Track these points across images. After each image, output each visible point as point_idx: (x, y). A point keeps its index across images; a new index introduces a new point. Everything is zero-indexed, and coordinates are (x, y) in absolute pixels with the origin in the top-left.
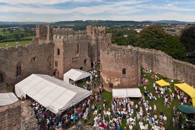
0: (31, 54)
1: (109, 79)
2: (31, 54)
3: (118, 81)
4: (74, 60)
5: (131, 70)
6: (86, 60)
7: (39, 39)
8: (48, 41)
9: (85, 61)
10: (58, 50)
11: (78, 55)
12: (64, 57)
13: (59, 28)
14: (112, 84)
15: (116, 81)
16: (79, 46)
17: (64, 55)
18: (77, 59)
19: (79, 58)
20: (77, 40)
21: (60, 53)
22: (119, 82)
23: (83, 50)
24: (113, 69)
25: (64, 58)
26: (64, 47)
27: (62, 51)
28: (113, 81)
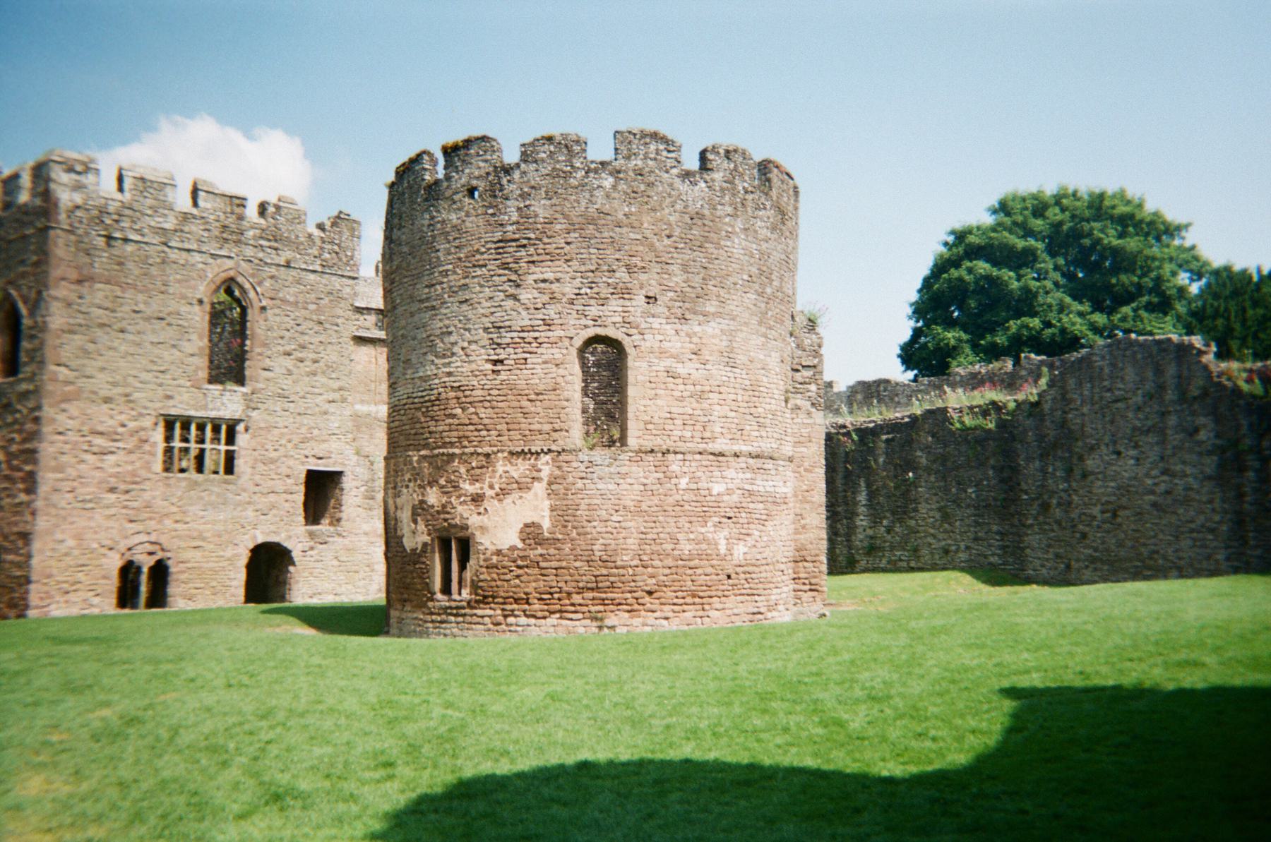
1: (433, 497)
3: (522, 487)
5: (681, 370)
9: (321, 490)
11: (226, 402)
14: (465, 546)
15: (502, 494)
22: (535, 507)
23: (289, 362)
24: (480, 358)
28: (477, 499)
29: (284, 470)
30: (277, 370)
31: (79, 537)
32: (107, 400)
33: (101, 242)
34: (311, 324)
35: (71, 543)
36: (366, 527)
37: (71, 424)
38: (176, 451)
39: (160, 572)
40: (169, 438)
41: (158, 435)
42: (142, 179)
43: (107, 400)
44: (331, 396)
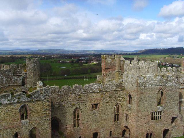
0: (91, 99)
2: (91, 99)
4: (153, 116)
6: (176, 118)
7: (105, 77)
8: (115, 82)
10: (130, 96)
11: (160, 108)
12: (138, 109)
13: (135, 60)
16: (164, 94)
17: (138, 106)
18: (160, 115)
19: (162, 114)
20: (161, 82)
21: (132, 101)
23: (169, 101)
25: (138, 111)
26: (138, 92)
27: (135, 98)
29: (168, 118)
30: (168, 102)
31: (141, 131)
32: (145, 111)
33: (143, 87)
34: (172, 94)
35: (140, 132)
36: (181, 125)
37: (140, 115)
38: (153, 117)
39: (151, 134)
40: (152, 115)
41: (151, 115)
42: (149, 76)
43: (145, 111)
44: (176, 105)
